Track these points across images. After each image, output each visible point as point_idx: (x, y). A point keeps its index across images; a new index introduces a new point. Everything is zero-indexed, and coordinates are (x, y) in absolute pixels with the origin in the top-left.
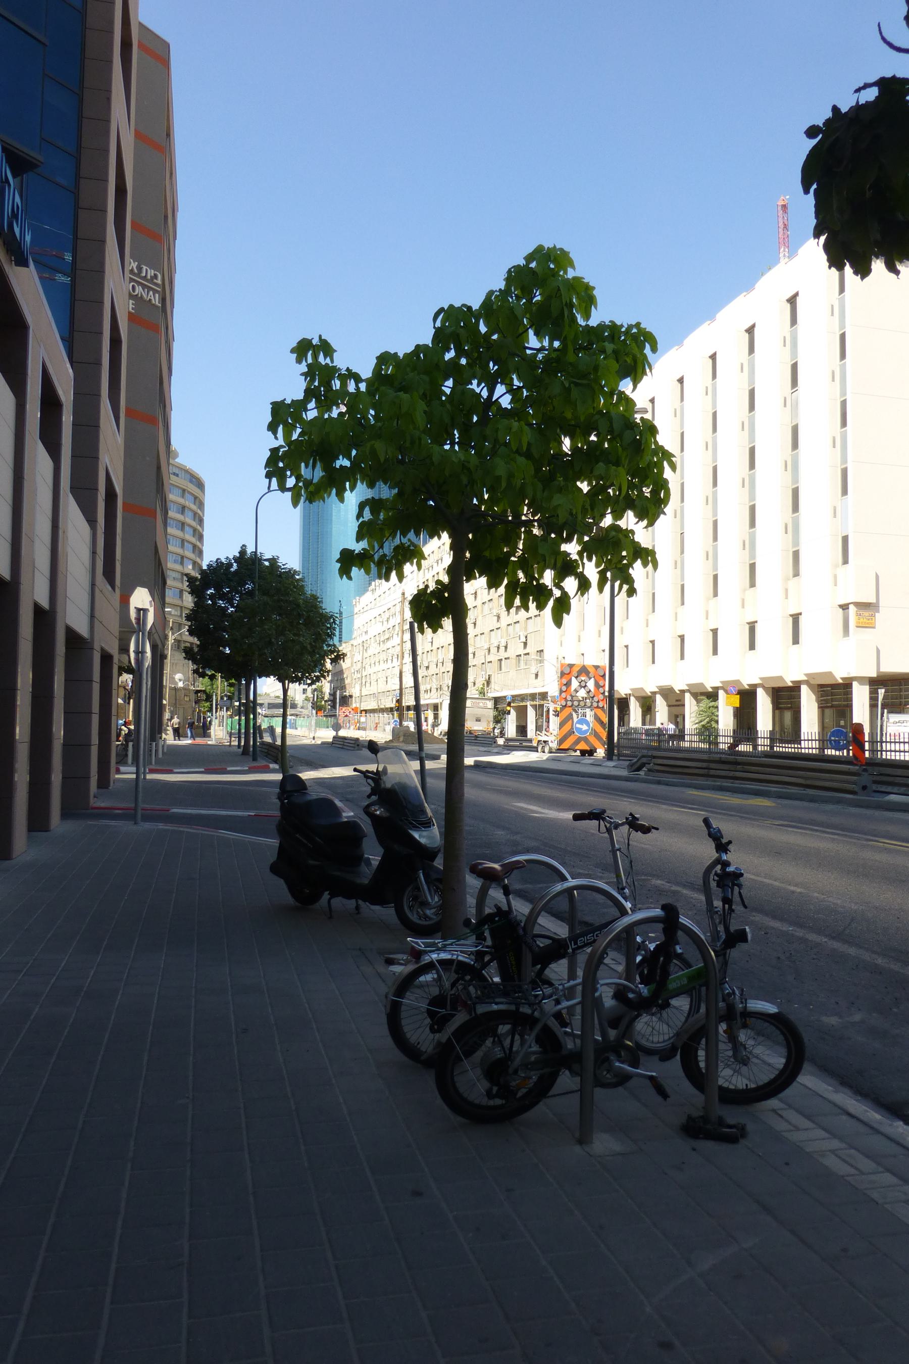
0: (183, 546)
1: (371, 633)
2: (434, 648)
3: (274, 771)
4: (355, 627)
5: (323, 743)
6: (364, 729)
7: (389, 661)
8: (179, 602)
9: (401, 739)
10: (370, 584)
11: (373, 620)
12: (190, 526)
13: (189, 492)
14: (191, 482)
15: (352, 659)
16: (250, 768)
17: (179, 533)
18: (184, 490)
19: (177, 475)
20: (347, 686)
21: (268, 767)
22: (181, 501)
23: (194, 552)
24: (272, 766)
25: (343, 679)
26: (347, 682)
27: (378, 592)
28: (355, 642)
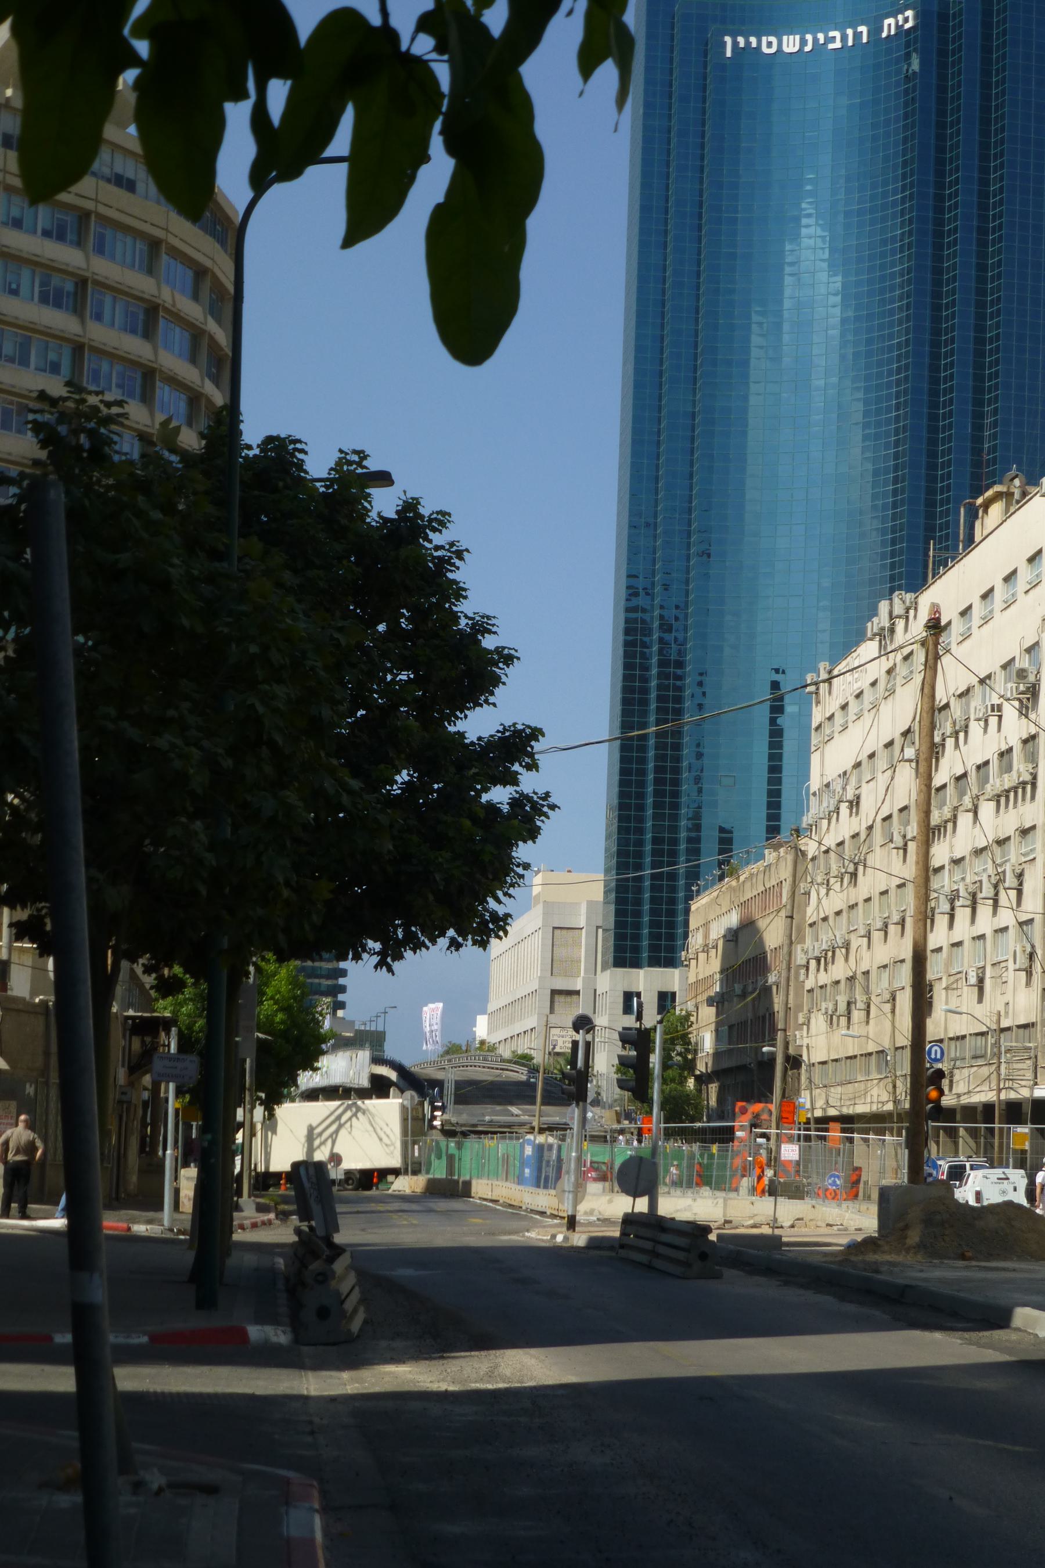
3: (50, 1356)
4: (815, 783)
5: (596, 1244)
6: (796, 1192)
9: (914, 1237)
11: (881, 763)
12: (174, 382)
13: (176, 253)
16: (154, 1338)
18: (155, 245)
19: (130, 186)
21: (243, 1335)
22: (143, 284)
24: (254, 1332)
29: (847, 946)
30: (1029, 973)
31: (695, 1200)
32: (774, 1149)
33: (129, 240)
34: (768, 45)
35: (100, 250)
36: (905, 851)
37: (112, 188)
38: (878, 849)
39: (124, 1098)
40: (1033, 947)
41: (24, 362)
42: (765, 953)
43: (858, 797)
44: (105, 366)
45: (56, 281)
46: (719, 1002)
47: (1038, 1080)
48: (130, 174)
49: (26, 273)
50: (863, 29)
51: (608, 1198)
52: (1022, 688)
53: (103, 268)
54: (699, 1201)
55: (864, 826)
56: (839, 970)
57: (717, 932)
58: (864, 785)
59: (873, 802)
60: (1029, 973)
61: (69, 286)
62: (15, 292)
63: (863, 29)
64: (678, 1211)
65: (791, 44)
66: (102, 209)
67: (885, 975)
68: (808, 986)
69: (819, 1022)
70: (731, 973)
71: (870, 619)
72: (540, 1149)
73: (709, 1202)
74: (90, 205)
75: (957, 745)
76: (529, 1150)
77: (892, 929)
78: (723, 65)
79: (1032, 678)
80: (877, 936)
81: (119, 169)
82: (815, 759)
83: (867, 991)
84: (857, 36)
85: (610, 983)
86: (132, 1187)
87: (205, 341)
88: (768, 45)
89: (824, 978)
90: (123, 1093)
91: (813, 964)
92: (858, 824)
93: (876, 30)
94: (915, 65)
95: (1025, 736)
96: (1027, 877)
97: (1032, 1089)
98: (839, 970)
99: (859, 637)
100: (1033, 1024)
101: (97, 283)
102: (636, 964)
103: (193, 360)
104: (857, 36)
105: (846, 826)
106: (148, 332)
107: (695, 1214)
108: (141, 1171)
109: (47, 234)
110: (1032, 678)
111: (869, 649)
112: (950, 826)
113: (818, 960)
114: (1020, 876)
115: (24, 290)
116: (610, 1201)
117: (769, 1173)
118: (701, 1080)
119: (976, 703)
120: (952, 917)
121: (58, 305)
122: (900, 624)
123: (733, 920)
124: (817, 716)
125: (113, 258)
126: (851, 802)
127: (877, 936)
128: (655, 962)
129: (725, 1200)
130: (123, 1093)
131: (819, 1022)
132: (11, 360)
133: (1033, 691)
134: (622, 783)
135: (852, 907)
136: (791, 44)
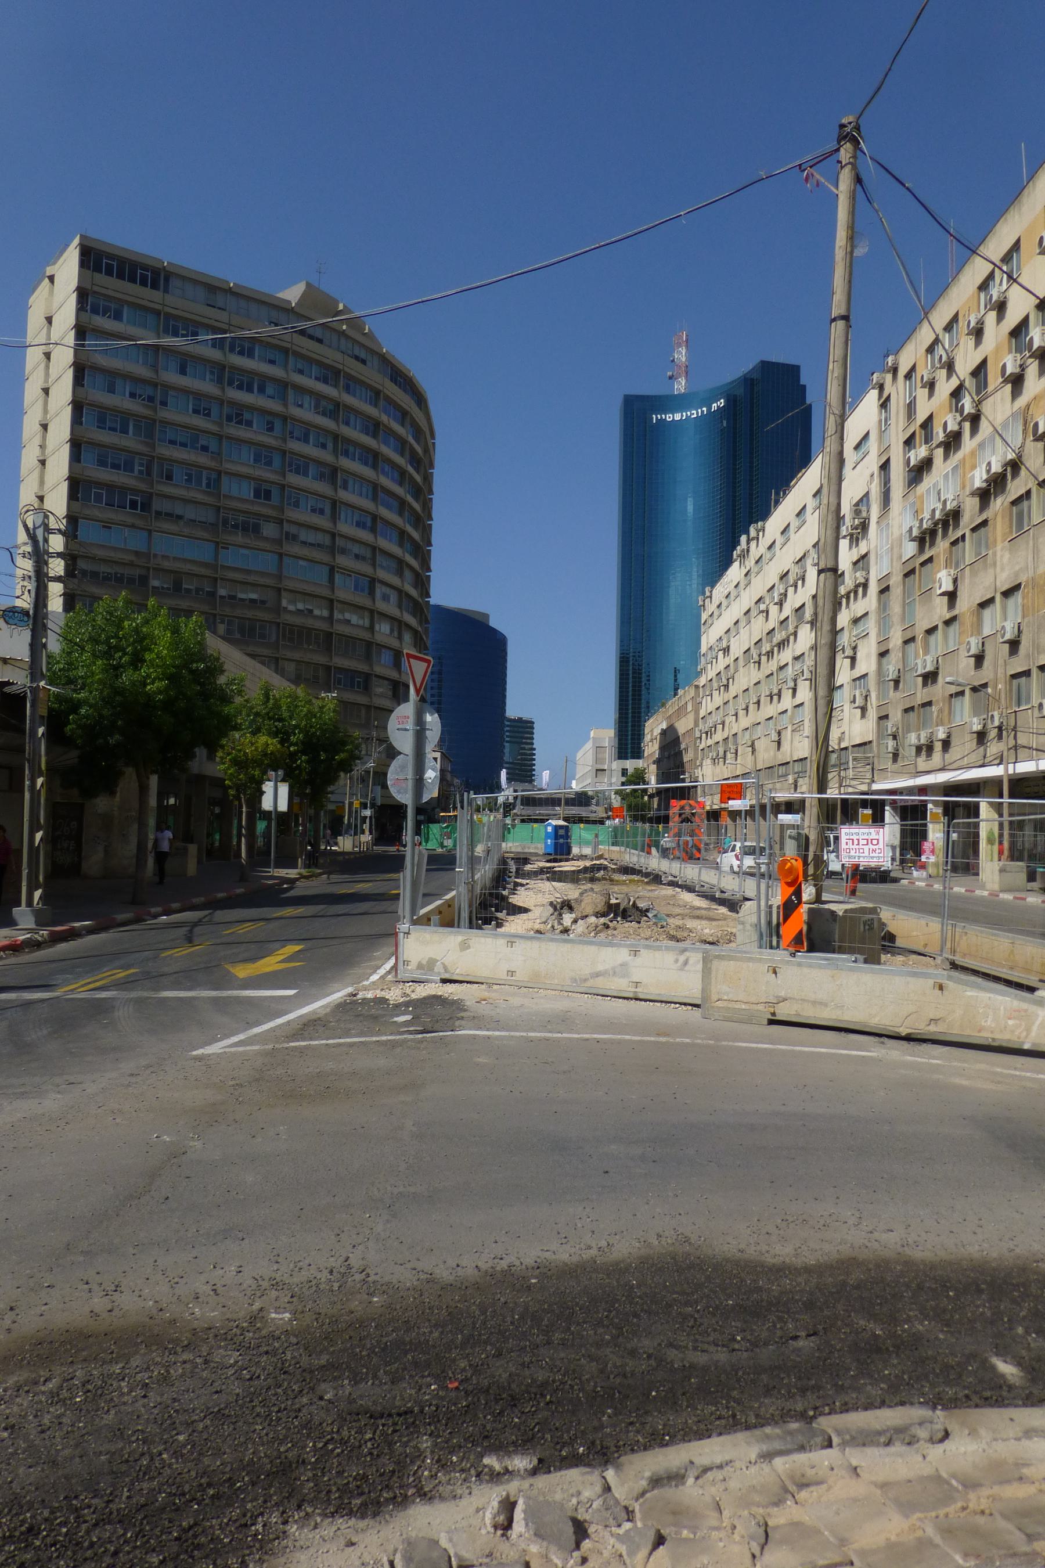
0: (375, 499)
1: (736, 650)
2: (965, 603)
4: (704, 649)
6: (874, 943)
7: (787, 695)
8: (367, 602)
10: (737, 543)
11: (742, 624)
13: (389, 400)
14: (393, 379)
15: (697, 712)
17: (367, 472)
18: (377, 393)
19: (364, 362)
20: (687, 766)
22: (372, 411)
23: (401, 514)
25: (679, 754)
26: (686, 758)
27: (755, 551)
28: (702, 681)
29: (723, 723)
30: (864, 710)
31: (636, 953)
32: (813, 837)
33: (364, 389)
34: (669, 417)
35: (347, 389)
36: (759, 663)
37: (353, 360)
38: (741, 669)
40: (868, 691)
41: (306, 440)
42: (678, 737)
43: (728, 647)
44: (351, 449)
45: (323, 403)
46: (658, 762)
47: (875, 779)
48: (363, 355)
49: (307, 399)
50: (705, 409)
51: (460, 938)
52: (857, 522)
53: (348, 399)
55: (732, 659)
56: (719, 736)
57: (657, 731)
58: (732, 639)
59: (738, 645)
60: (864, 710)
61: (331, 407)
62: (301, 406)
63: (705, 409)
64: (597, 975)
66: (346, 369)
67: (747, 733)
68: (701, 747)
69: (708, 762)
70: (662, 748)
71: (734, 548)
72: (557, 828)
73: (669, 958)
74: (341, 367)
75: (796, 591)
76: (550, 829)
77: (752, 707)
78: (653, 426)
79: (864, 514)
80: (741, 713)
81: (357, 352)
82: (704, 639)
83: (736, 743)
84: (702, 412)
85: (617, 765)
87: (408, 446)
88: (669, 417)
89: (710, 742)
91: (704, 735)
92: (729, 660)
94: (725, 423)
95: (855, 559)
96: (859, 648)
97: (870, 785)
98: (719, 736)
99: (726, 563)
100: (870, 742)
101: (345, 406)
102: (627, 759)
103: (402, 455)
104: (702, 412)
105: (722, 662)
106: (375, 436)
107: (637, 984)
109: (317, 379)
110: (864, 514)
111: (736, 564)
112: (792, 638)
113: (707, 733)
114: (855, 648)
115: (306, 405)
116: (464, 946)
117: (808, 892)
118: (651, 796)
119: (809, 562)
120: (794, 690)
121: (324, 414)
122: (753, 544)
123: (664, 726)
124: (704, 616)
125: (355, 396)
126: (724, 649)
127: (741, 713)
128: (633, 758)
129: (706, 961)
131: (708, 762)
132: (299, 439)
133: (864, 526)
134: (620, 688)
135: (725, 703)
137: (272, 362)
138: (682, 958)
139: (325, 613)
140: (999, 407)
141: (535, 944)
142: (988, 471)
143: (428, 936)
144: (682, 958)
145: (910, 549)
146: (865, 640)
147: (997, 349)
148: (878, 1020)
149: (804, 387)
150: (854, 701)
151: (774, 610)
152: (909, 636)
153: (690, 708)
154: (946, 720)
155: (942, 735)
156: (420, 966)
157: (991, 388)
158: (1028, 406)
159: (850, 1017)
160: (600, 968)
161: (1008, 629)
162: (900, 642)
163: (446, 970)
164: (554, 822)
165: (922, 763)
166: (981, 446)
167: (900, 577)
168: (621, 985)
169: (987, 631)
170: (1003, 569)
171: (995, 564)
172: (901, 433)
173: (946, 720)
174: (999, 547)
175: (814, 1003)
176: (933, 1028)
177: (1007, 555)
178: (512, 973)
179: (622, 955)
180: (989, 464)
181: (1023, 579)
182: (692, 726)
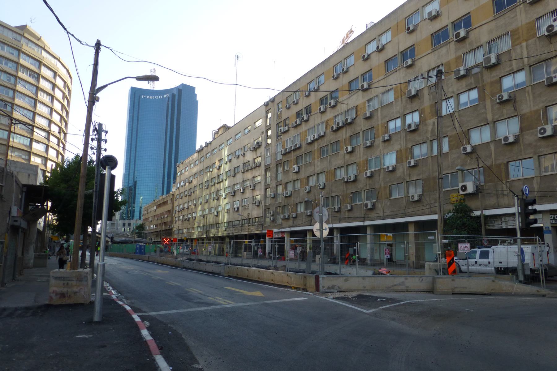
31: (406, 279)
34: (148, 97)
39: (16, 224)
51: (344, 278)
54: (410, 279)
65: (151, 97)
72: (141, 246)
76: (138, 246)
86: (30, 264)
88: (148, 97)
90: (17, 221)
93: (163, 97)
98: (185, 213)
107: (407, 287)
108: (35, 258)
130: (17, 221)
136: (151, 97)
137: (13, 54)
138: (421, 279)
139: (27, 157)
140: (316, 119)
141: (373, 278)
142: (314, 138)
143: (332, 278)
144: (421, 279)
145: (279, 157)
146: (259, 184)
147: (315, 102)
148: (480, 290)
149: (196, 95)
150: (255, 203)
151: (215, 171)
152: (279, 183)
153: (169, 202)
154: (295, 211)
155: (294, 216)
156: (329, 288)
157: (312, 114)
158: (327, 121)
159: (473, 290)
160: (395, 283)
161: (321, 185)
162: (275, 185)
163: (339, 288)
164: (140, 244)
165: (285, 223)
166: (309, 130)
167: (275, 165)
168: (403, 288)
169: (311, 184)
170: (318, 167)
171: (314, 165)
172: (275, 121)
173: (295, 211)
174: (316, 160)
175: (464, 288)
176: (492, 291)
177: (319, 163)
178: (364, 287)
179: (402, 279)
180: (314, 136)
181: (326, 170)
182: (170, 208)
